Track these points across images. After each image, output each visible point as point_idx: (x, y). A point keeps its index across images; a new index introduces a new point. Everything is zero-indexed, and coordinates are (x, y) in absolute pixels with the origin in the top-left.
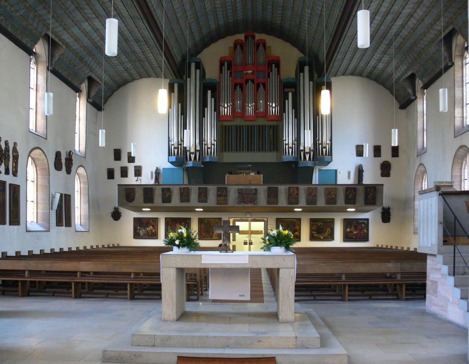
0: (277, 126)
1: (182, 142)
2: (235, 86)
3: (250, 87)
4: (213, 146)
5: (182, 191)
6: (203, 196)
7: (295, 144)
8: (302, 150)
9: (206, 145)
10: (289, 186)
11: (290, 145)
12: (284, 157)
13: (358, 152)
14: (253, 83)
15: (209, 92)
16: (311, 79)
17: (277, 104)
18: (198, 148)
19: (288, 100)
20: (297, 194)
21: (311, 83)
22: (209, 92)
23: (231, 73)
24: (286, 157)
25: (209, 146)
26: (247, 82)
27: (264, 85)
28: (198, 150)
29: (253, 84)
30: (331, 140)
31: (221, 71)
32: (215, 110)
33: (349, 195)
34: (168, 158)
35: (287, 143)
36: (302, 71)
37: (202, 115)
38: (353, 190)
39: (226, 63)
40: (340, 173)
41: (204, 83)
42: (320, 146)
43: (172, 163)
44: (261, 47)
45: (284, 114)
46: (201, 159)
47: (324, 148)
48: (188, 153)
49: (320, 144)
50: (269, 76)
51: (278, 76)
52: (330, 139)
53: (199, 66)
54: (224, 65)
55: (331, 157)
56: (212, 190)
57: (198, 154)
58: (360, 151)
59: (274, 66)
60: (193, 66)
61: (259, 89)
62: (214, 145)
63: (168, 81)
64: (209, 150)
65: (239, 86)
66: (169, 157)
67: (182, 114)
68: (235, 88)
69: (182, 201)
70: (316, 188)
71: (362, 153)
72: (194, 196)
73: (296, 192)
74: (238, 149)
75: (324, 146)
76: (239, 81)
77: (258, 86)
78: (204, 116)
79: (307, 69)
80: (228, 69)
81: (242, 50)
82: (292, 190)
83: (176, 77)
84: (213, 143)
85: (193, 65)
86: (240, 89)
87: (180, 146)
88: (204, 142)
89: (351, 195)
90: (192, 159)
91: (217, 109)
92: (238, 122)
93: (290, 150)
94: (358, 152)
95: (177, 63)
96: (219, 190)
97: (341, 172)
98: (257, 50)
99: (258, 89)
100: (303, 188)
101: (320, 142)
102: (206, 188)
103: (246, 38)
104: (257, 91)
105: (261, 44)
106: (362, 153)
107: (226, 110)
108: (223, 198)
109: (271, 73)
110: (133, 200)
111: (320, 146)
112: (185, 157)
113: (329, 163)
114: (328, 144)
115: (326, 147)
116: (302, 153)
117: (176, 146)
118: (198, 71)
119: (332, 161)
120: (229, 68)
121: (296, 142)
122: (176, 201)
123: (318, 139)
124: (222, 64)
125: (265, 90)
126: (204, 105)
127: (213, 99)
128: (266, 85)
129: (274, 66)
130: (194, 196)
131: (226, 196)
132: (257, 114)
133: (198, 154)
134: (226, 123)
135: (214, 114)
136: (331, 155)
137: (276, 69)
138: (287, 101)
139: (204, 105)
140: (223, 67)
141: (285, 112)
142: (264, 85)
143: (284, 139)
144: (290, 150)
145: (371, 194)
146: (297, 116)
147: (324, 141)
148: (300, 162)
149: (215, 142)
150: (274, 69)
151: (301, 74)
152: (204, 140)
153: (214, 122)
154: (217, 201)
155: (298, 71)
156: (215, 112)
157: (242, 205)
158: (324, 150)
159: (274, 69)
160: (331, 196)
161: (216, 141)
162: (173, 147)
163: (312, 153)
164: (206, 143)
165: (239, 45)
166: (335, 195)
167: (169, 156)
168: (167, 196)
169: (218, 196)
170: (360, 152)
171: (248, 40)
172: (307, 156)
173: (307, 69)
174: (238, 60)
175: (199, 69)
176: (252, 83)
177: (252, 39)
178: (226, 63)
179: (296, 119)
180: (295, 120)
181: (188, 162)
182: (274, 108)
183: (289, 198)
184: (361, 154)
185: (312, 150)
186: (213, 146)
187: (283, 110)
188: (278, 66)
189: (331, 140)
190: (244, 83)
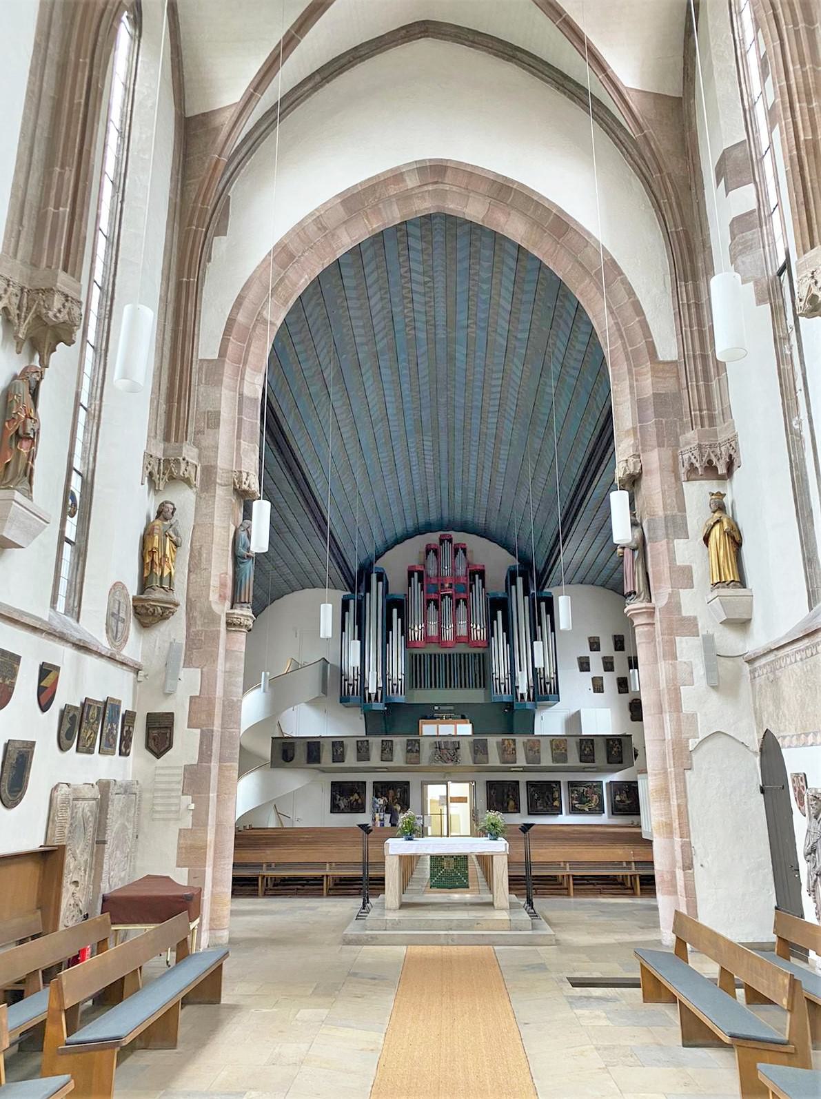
0: (483, 654)
2: (429, 602)
3: (447, 604)
4: (400, 682)
5: (360, 745)
6: (387, 750)
11: (502, 681)
14: (452, 598)
15: (395, 611)
18: (380, 685)
20: (514, 749)
22: (395, 611)
23: (422, 586)
25: (395, 682)
26: (443, 597)
27: (465, 601)
31: (410, 585)
32: (402, 634)
33: (585, 749)
35: (497, 677)
36: (514, 582)
37: (386, 640)
38: (589, 743)
39: (416, 574)
42: (542, 681)
44: (461, 551)
47: (548, 683)
53: (381, 577)
56: (399, 742)
59: (477, 576)
60: (374, 576)
62: (401, 680)
63: (340, 594)
64: (395, 687)
68: (428, 606)
69: (359, 760)
70: (539, 741)
72: (375, 753)
73: (512, 746)
74: (434, 685)
76: (433, 596)
78: (388, 642)
79: (520, 580)
80: (419, 581)
82: (506, 742)
84: (400, 677)
85: (374, 576)
87: (356, 682)
89: (587, 749)
91: (404, 631)
92: (433, 649)
93: (503, 687)
96: (409, 743)
99: (457, 606)
100: (520, 740)
101: (542, 676)
102: (392, 741)
103: (442, 541)
107: (417, 632)
108: (415, 754)
110: (292, 759)
111: (542, 681)
117: (351, 682)
118: (380, 583)
120: (420, 580)
122: (351, 759)
124: (411, 574)
126: (388, 627)
127: (400, 620)
129: (477, 576)
130: (375, 753)
131: (418, 751)
132: (457, 639)
134: (416, 651)
136: (558, 693)
138: (495, 622)
139: (388, 627)
141: (493, 635)
142: (465, 601)
144: (503, 687)
145: (615, 749)
146: (509, 640)
150: (478, 582)
151: (513, 587)
154: (407, 758)
155: (509, 583)
157: (440, 764)
158: (548, 686)
159: (478, 582)
160: (559, 751)
166: (566, 750)
168: (339, 753)
169: (408, 751)
173: (520, 580)
174: (432, 571)
175: (382, 581)
178: (416, 574)
182: (479, 633)
183: (503, 754)
187: (490, 633)
188: (482, 574)
189: (556, 673)
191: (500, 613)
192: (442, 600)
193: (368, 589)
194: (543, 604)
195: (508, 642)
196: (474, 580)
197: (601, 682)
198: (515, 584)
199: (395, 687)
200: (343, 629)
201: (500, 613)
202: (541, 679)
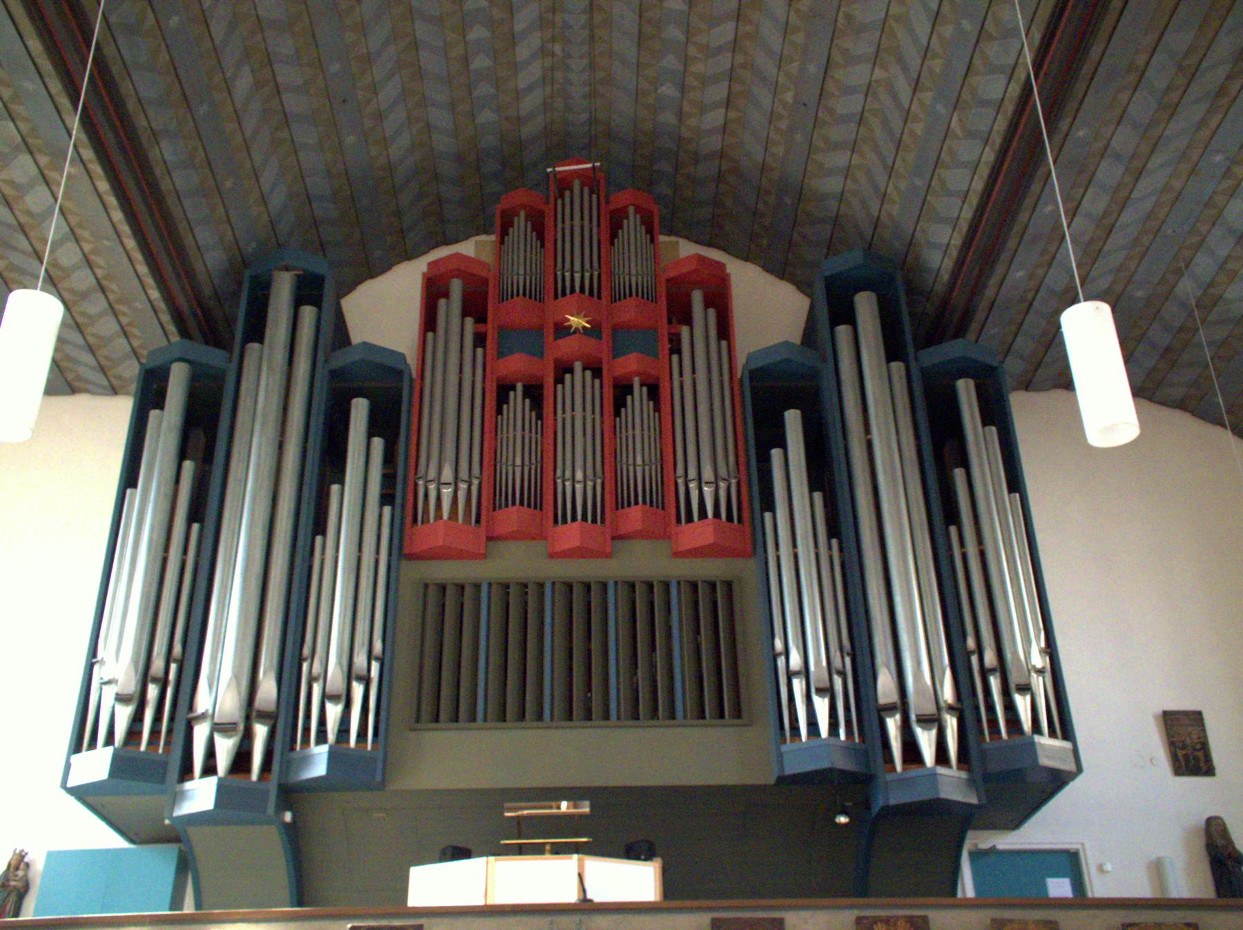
1: (173, 667)
2: (503, 391)
7: (842, 674)
8: (890, 709)
9: (316, 679)
10: (856, 913)
12: (788, 747)
13: (1180, 753)
14: (597, 373)
15: (360, 410)
16: (893, 351)
17: (723, 471)
19: (783, 445)
21: (898, 367)
22: (360, 410)
23: (480, 340)
24: (794, 746)
26: (563, 369)
27: (654, 392)
28: (264, 716)
29: (597, 382)
30: (1051, 649)
31: (429, 322)
32: (387, 498)
34: (68, 766)
36: (843, 313)
39: (456, 287)
40: (1100, 868)
41: (333, 374)
42: (994, 682)
43: (84, 794)
45: (768, 515)
46: (276, 767)
48: (201, 733)
49: (993, 670)
50: (676, 349)
51: (724, 343)
52: (1043, 644)
54: (446, 295)
55: (1067, 745)
57: (261, 731)
58: (1188, 741)
59: (697, 298)
61: (625, 405)
64: (334, 712)
65: (519, 386)
66: (75, 758)
67: (196, 513)
71: (1200, 754)
75: (1014, 679)
77: (622, 391)
78: (320, 527)
79: (865, 305)
81: (541, 237)
83: (184, 333)
86: (527, 401)
88: (305, 666)
90: (223, 761)
94: (1180, 753)
95: (202, 276)
97: (1108, 867)
98: (614, 236)
99: (619, 404)
101: (990, 658)
104: (617, 413)
105: (631, 210)
106: (1200, 754)
109: (685, 331)
111: (994, 682)
112: (177, 753)
113: (1057, 780)
114: (1040, 672)
115: (1025, 688)
116: (893, 725)
118: (308, 312)
119: (1079, 770)
120: (475, 307)
121: (848, 660)
123: (971, 643)
125: (657, 409)
127: (378, 443)
128: (664, 385)
129: (697, 298)
133: (261, 731)
135: (379, 518)
137: (712, 312)
140: (442, 302)
141: (769, 505)
143: (779, 645)
144: (822, 706)
147: (1015, 652)
148: (889, 777)
149: (375, 666)
151: (843, 331)
152: (306, 651)
153: (377, 554)
156: (387, 510)
158: (1022, 704)
161: (382, 661)
162: (109, 694)
163: (951, 723)
164: (317, 668)
165: (522, 214)
167: (77, 747)
170: (1189, 751)
171: (567, 193)
172: (926, 740)
173: (865, 305)
176: (588, 373)
177: (586, 190)
178: (456, 287)
179: (834, 542)
180: (830, 548)
181: (188, 785)
184: (1195, 758)
185: (951, 708)
186: (358, 690)
189: (1051, 649)
190: (550, 380)
191: (793, 420)
192: (559, 380)
193: (256, 331)
194: (966, 390)
195: (833, 530)
196: (688, 320)
197: (1195, 732)
198: (849, 318)
199: (334, 712)
200: (130, 478)
201: (793, 420)
202: (984, 673)
